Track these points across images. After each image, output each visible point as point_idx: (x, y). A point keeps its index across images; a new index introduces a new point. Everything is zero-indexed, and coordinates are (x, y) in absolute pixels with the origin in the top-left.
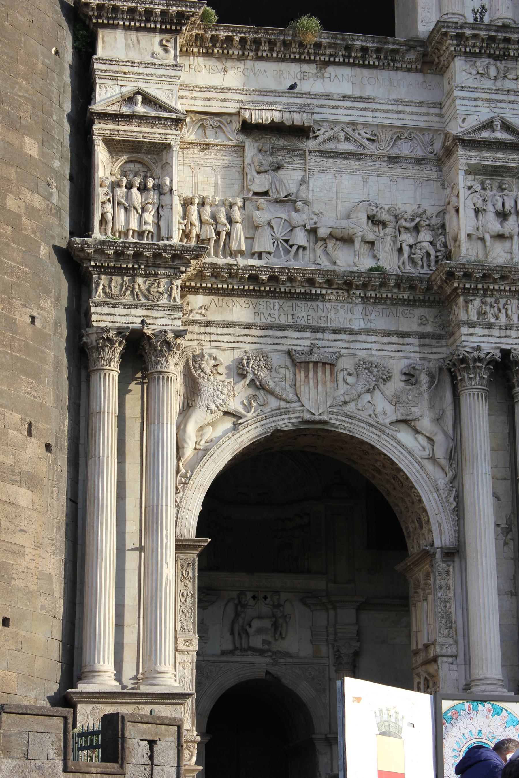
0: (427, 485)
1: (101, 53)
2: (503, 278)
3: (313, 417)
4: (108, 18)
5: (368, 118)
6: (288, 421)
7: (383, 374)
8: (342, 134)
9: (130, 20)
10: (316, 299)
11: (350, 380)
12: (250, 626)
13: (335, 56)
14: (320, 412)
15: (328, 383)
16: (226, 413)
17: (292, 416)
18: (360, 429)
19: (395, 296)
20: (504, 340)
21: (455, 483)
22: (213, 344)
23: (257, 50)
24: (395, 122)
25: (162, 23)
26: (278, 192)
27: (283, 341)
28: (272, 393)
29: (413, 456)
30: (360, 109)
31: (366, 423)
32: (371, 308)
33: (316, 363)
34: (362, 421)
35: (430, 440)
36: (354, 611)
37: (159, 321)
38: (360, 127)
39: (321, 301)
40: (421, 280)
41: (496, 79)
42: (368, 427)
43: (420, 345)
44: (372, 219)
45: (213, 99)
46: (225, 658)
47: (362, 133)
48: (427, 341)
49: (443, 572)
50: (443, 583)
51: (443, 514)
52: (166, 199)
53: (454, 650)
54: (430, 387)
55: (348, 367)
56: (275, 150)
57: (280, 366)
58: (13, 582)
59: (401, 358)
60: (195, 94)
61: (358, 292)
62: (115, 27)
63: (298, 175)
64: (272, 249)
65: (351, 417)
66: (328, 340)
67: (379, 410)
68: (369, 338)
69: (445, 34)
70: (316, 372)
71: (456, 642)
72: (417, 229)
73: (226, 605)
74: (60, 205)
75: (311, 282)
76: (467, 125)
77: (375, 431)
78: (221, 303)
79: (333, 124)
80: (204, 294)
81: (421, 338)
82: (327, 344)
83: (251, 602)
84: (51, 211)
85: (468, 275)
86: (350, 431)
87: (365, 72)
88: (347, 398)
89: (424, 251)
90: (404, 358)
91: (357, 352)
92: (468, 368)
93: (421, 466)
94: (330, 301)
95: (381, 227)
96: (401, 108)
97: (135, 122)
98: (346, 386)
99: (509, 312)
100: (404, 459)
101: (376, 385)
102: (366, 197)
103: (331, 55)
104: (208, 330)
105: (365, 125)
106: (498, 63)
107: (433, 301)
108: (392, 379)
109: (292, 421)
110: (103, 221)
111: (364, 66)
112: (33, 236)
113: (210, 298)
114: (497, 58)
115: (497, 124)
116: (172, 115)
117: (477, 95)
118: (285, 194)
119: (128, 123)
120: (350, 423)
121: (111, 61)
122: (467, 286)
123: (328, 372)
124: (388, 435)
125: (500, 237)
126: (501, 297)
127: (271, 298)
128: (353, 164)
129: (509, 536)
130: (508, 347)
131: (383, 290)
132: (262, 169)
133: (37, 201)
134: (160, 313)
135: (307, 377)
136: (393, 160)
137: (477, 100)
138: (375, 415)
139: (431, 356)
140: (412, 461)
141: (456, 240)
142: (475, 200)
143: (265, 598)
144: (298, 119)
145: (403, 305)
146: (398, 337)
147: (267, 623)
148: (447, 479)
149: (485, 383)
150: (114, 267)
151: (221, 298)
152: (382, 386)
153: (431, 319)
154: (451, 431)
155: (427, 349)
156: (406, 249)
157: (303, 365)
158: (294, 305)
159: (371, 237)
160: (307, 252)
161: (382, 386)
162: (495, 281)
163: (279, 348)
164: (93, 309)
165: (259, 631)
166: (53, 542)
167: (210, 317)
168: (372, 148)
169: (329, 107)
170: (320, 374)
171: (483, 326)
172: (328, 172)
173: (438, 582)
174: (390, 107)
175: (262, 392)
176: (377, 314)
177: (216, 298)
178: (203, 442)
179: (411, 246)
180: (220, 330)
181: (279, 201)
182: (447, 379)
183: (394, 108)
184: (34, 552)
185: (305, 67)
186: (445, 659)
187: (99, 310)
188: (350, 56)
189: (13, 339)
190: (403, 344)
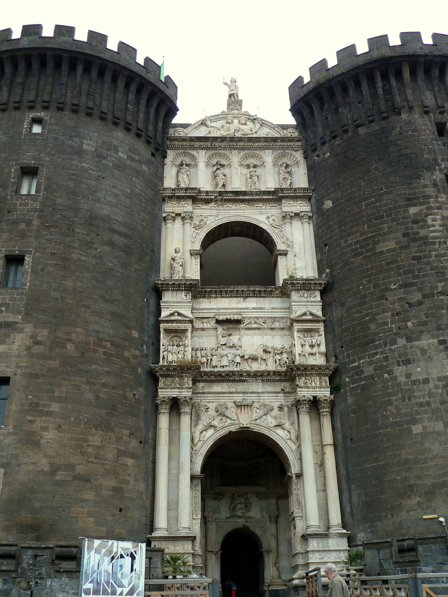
1: (163, 299)
2: (312, 369)
3: (244, 426)
4: (166, 287)
5: (262, 315)
8: (253, 321)
9: (174, 287)
11: (258, 411)
12: (236, 507)
13: (250, 294)
16: (211, 426)
20: (314, 393)
21: (300, 448)
23: (221, 294)
24: (273, 316)
26: (230, 344)
27: (232, 398)
28: (228, 418)
29: (283, 439)
30: (259, 312)
31: (264, 427)
33: (244, 405)
35: (289, 432)
36: (275, 500)
37: (183, 393)
38: (260, 318)
40: (282, 372)
41: (307, 297)
43: (284, 396)
44: (265, 351)
45: (206, 313)
46: (227, 520)
47: (261, 320)
48: (287, 395)
50: (296, 488)
52: (187, 349)
53: (301, 514)
56: (228, 329)
58: (125, 495)
59: (277, 401)
60: (199, 311)
61: (260, 378)
62: (168, 290)
63: (237, 337)
64: (228, 364)
65: (258, 425)
67: (269, 421)
68: (264, 395)
69: (287, 283)
70: (244, 409)
71: (302, 511)
72: (282, 353)
73: (227, 500)
74: (147, 353)
75: (242, 375)
76: (296, 315)
79: (250, 318)
80: (202, 382)
82: (248, 398)
83: (237, 498)
85: (298, 369)
87: (261, 299)
88: (257, 418)
89: (284, 361)
90: (278, 401)
92: (300, 404)
93: (286, 442)
94: (249, 382)
96: (274, 310)
97: (175, 322)
102: (263, 343)
103: (248, 294)
104: (204, 395)
105: (262, 318)
106: (308, 292)
107: (289, 379)
110: (164, 358)
111: (260, 297)
113: (205, 383)
114: (307, 290)
115: (308, 313)
116: (188, 319)
117: (300, 304)
119: (172, 323)
121: (167, 302)
122: (299, 373)
123: (249, 408)
124: (273, 431)
125: (312, 354)
126: (313, 376)
127: (228, 382)
128: (258, 331)
129: (322, 468)
130: (316, 395)
131: (269, 376)
132: (224, 336)
133: (137, 353)
135: (241, 411)
136: (272, 329)
137: (300, 305)
141: (295, 356)
142: (301, 341)
143: (242, 496)
144: (236, 317)
145: (277, 382)
147: (243, 506)
148: (296, 447)
149: (307, 409)
150: (167, 374)
152: (270, 413)
153: (288, 386)
154: (297, 429)
155: (287, 398)
156: (277, 361)
159: (264, 358)
160: (241, 365)
161: (270, 413)
162: (309, 371)
163: (230, 400)
164: (159, 390)
165: (240, 509)
167: (205, 391)
168: (265, 326)
169: (248, 312)
170: (246, 409)
171: (305, 388)
172: (249, 335)
174: (270, 311)
177: (207, 384)
179: (279, 360)
180: (208, 395)
181: (230, 347)
182: (294, 408)
184: (134, 483)
185: (239, 299)
186: (298, 518)
187: (161, 390)
188: (255, 294)
189: (126, 402)
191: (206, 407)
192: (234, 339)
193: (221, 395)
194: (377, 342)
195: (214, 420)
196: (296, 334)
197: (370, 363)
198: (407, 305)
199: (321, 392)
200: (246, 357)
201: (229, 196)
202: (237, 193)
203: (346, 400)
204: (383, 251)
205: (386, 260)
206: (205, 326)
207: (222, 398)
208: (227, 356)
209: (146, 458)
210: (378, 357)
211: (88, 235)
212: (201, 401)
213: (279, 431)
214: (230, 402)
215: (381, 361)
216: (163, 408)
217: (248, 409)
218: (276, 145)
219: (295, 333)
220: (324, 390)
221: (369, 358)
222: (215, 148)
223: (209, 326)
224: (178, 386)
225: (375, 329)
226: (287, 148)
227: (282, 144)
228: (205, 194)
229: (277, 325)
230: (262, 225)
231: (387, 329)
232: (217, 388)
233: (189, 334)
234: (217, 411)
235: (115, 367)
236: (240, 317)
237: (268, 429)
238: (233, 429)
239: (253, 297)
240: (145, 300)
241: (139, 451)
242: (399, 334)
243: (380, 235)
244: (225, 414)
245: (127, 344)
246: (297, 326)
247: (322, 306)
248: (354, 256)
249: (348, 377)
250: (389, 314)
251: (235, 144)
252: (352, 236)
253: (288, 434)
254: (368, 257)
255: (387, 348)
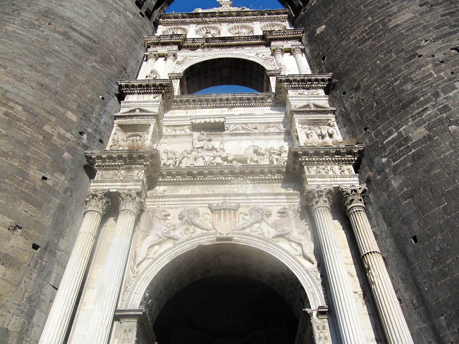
0: (301, 270)
3: (222, 236)
5: (252, 121)
6: (207, 240)
7: (266, 212)
10: (226, 184)
11: (246, 217)
14: (227, 233)
15: (232, 219)
16: (170, 238)
17: (210, 237)
18: (253, 242)
19: (270, 177)
22: (166, 206)
25: (154, 89)
28: (198, 226)
32: (257, 185)
33: (225, 209)
34: (254, 237)
39: (229, 184)
42: (258, 240)
43: (287, 199)
44: (255, 152)
47: (250, 126)
48: (291, 197)
49: (320, 327)
50: (322, 335)
51: (314, 287)
54: (295, 217)
55: (245, 211)
57: (204, 214)
59: (276, 206)
60: (171, 119)
62: (133, 94)
66: (233, 200)
67: (265, 231)
68: (256, 197)
70: (225, 215)
74: (88, 145)
77: (262, 241)
78: (173, 189)
81: (287, 196)
84: (79, 144)
85: (306, 154)
86: (247, 243)
88: (244, 226)
90: (279, 205)
91: (250, 204)
94: (234, 184)
95: (261, 156)
96: (267, 116)
98: (244, 221)
99: (334, 170)
100: (283, 256)
101: (262, 219)
104: (164, 200)
106: (308, 91)
108: (272, 216)
109: (210, 239)
111: (250, 106)
112: (60, 146)
113: (167, 187)
116: (152, 114)
118: (212, 147)
120: (246, 238)
121: (129, 102)
122: (307, 159)
123: (232, 214)
124: (271, 243)
127: (201, 184)
128: (246, 137)
130: (338, 186)
132: (200, 139)
134: (129, 184)
135: (220, 217)
137: (300, 100)
138: (263, 234)
139: (294, 204)
140: (289, 256)
146: (273, 196)
151: (173, 187)
152: (266, 219)
157: (217, 211)
158: (214, 187)
161: (266, 219)
163: (204, 205)
166: (19, 307)
167: (166, 194)
172: (234, 140)
173: (317, 334)
175: (192, 226)
176: (261, 187)
178: (152, 255)
180: (170, 199)
183: (265, 116)
185: (223, 109)
189: (22, 181)
190: (277, 199)
191: (165, 213)
192: (216, 144)
193: (189, 199)
194: (422, 99)
195: (175, 230)
196: (298, 126)
197: (418, 125)
198: (453, 51)
199: (344, 183)
200: (230, 158)
201: (216, 42)
202: (224, 39)
203: (388, 185)
204: (399, 24)
205: (405, 28)
206: (178, 132)
207: (191, 202)
208: (204, 159)
209: (39, 275)
210: (429, 112)
211: (37, 20)
212: (158, 207)
213: (283, 244)
214: (203, 207)
215: (437, 115)
216: (91, 206)
217: (230, 214)
218: (264, 17)
219: (297, 124)
220: (348, 179)
221: (414, 120)
222: (206, 22)
223: (183, 132)
224: (122, 178)
225: (412, 88)
226: (274, 19)
227: (269, 16)
228: (191, 42)
229: (272, 130)
230: (251, 59)
231: (431, 80)
232: (184, 191)
233: (151, 129)
234: (181, 219)
235: (20, 133)
236: (222, 120)
237: (264, 240)
238: (206, 241)
239: (241, 106)
240: (101, 97)
241: (26, 258)
242: (455, 78)
243: (390, 15)
244: (193, 221)
245: (54, 119)
246: (297, 118)
247: (329, 100)
248: (359, 45)
249: (384, 157)
250: (430, 66)
251: (224, 18)
252: (354, 33)
253: (299, 248)
254: (380, 36)
255: (441, 98)
